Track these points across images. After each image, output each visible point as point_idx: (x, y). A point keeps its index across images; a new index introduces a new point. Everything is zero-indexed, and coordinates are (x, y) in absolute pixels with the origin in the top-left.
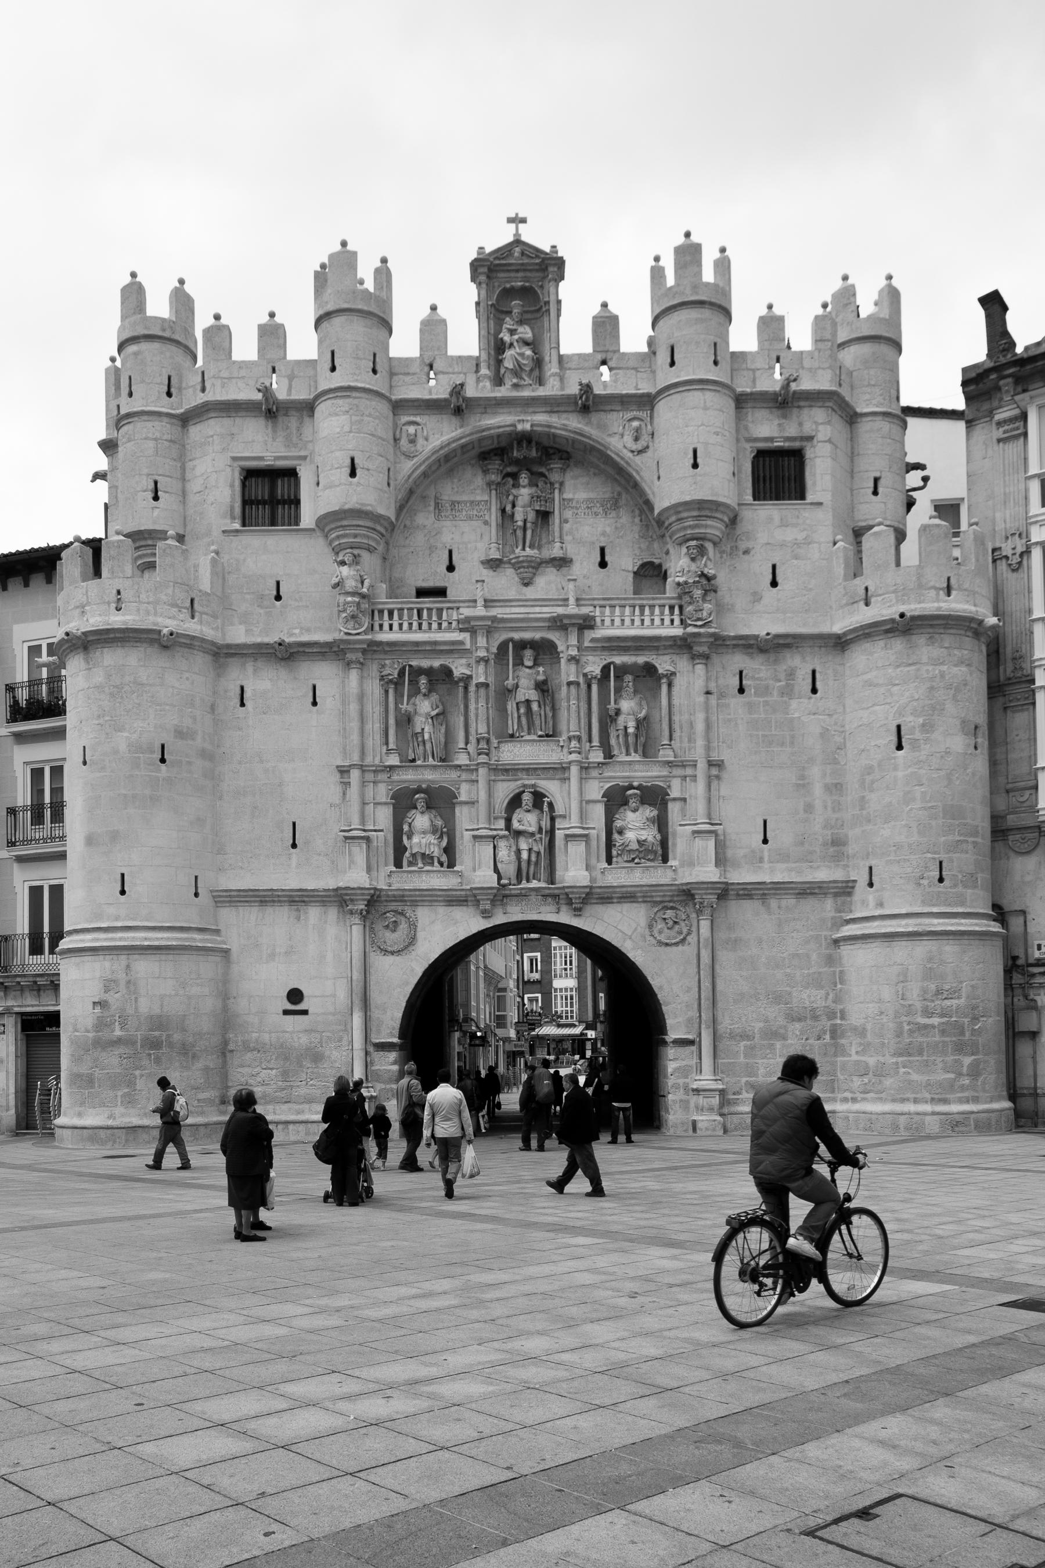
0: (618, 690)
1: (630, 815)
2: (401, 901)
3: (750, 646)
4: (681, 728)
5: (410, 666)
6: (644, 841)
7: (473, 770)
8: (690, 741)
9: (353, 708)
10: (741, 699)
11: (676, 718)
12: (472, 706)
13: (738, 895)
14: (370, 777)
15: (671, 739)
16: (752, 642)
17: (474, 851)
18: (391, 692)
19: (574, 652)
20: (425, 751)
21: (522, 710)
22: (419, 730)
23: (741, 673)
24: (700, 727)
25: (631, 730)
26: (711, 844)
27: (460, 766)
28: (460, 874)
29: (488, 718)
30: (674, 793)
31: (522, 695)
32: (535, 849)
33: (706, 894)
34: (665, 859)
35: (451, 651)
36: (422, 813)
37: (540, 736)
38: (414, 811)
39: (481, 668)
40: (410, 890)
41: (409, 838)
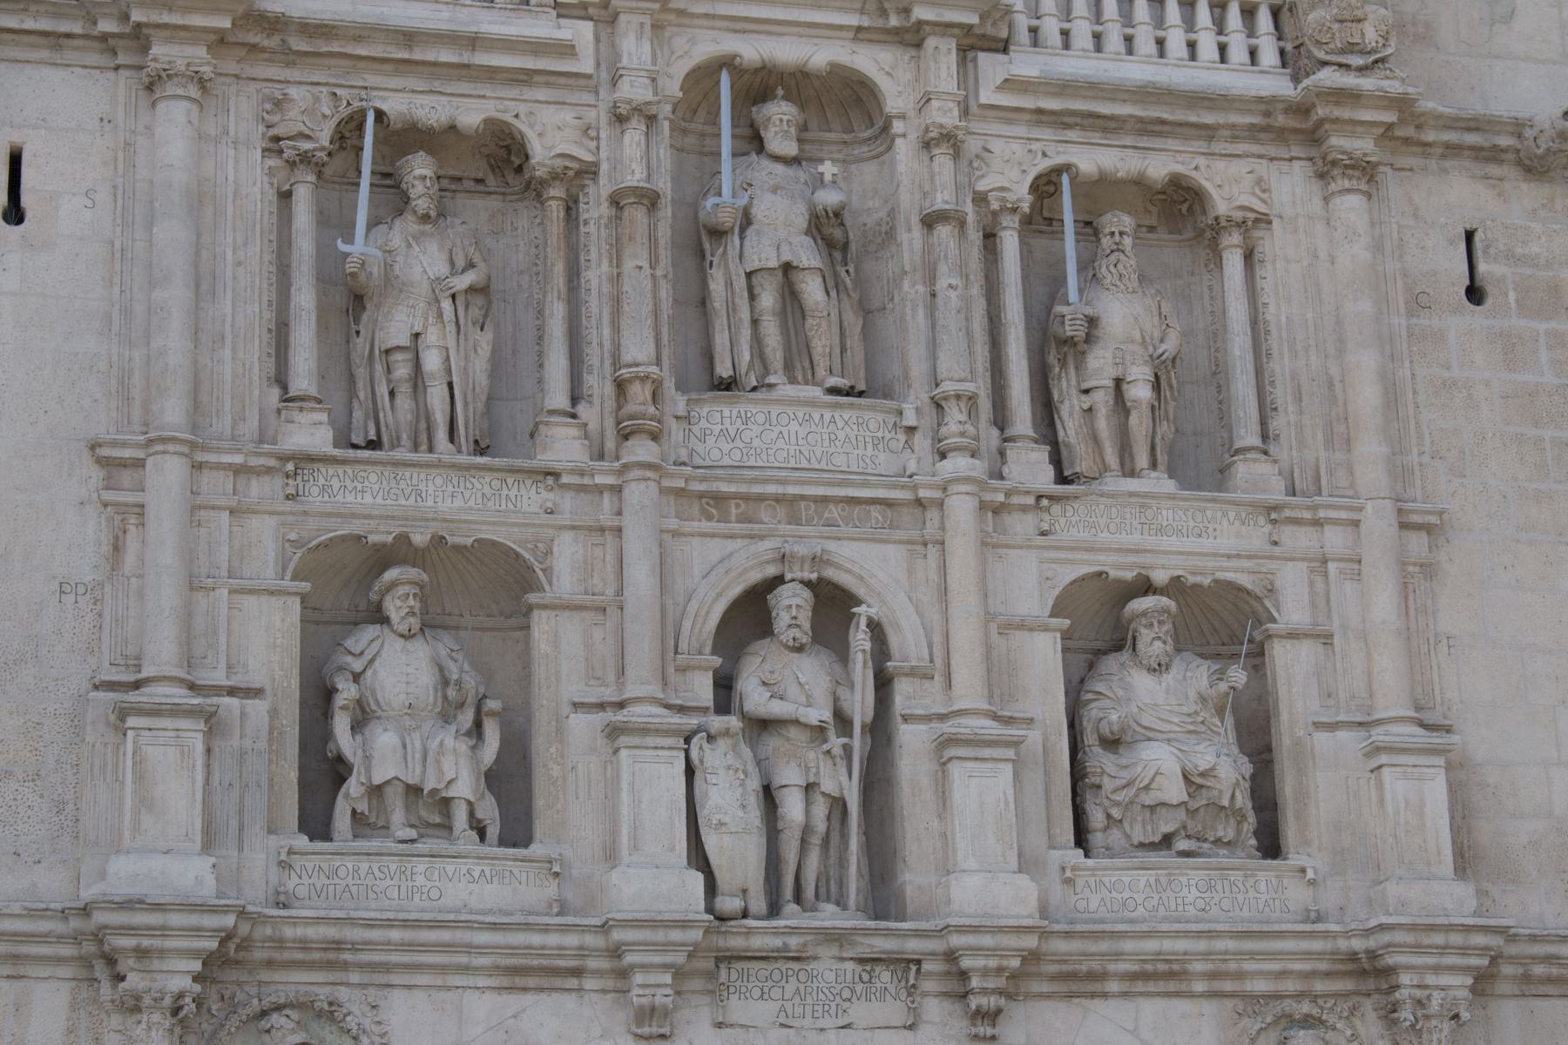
0: (1087, 266)
1: (1143, 684)
2: (330, 965)
3: (1492, 155)
4: (1299, 399)
5: (380, 115)
6: (1202, 775)
7: (599, 490)
8: (1329, 443)
9: (172, 235)
10: (1476, 317)
11: (1280, 366)
12: (596, 275)
13: (1527, 978)
14: (216, 486)
15: (1265, 437)
16: (1504, 141)
17: (613, 786)
18: (304, 197)
19: (945, 115)
20: (423, 415)
21: (768, 299)
22: (404, 340)
23: (1469, 236)
24: (1366, 396)
25: (1140, 392)
26: (1436, 791)
27: (555, 475)
28: (555, 871)
29: (656, 314)
30: (1293, 609)
31: (762, 251)
32: (828, 786)
33: (1437, 969)
34: (1271, 846)
35: (525, 78)
36: (407, 636)
37: (834, 391)
38: (372, 631)
39: (634, 134)
40: (370, 924)
41: (359, 724)
